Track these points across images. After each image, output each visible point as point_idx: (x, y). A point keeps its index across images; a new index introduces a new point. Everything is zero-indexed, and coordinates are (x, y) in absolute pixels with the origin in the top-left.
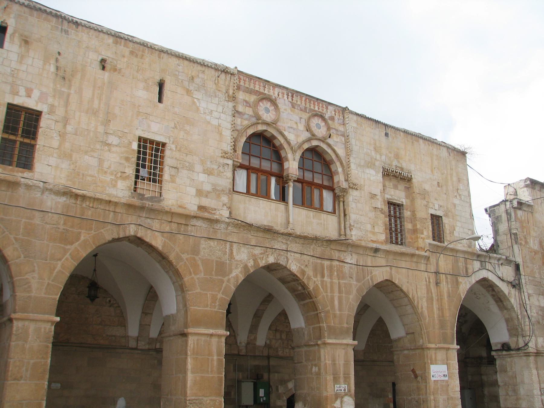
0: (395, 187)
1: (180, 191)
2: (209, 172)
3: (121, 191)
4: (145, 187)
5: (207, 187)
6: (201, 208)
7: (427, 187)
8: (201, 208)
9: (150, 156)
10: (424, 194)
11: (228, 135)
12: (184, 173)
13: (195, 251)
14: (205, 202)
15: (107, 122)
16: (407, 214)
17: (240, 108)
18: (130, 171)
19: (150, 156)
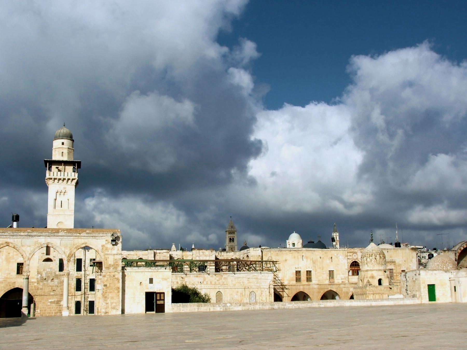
0: (391, 265)
1: (338, 279)
2: (343, 274)
3: (327, 282)
4: (331, 281)
5: (343, 277)
6: (342, 282)
7: (401, 263)
8: (342, 282)
9: (331, 273)
10: (400, 265)
11: (346, 265)
12: (338, 276)
13: (342, 290)
14: (343, 280)
15: (323, 269)
16: (394, 271)
17: (349, 257)
18: (328, 278)
19: (331, 273)
